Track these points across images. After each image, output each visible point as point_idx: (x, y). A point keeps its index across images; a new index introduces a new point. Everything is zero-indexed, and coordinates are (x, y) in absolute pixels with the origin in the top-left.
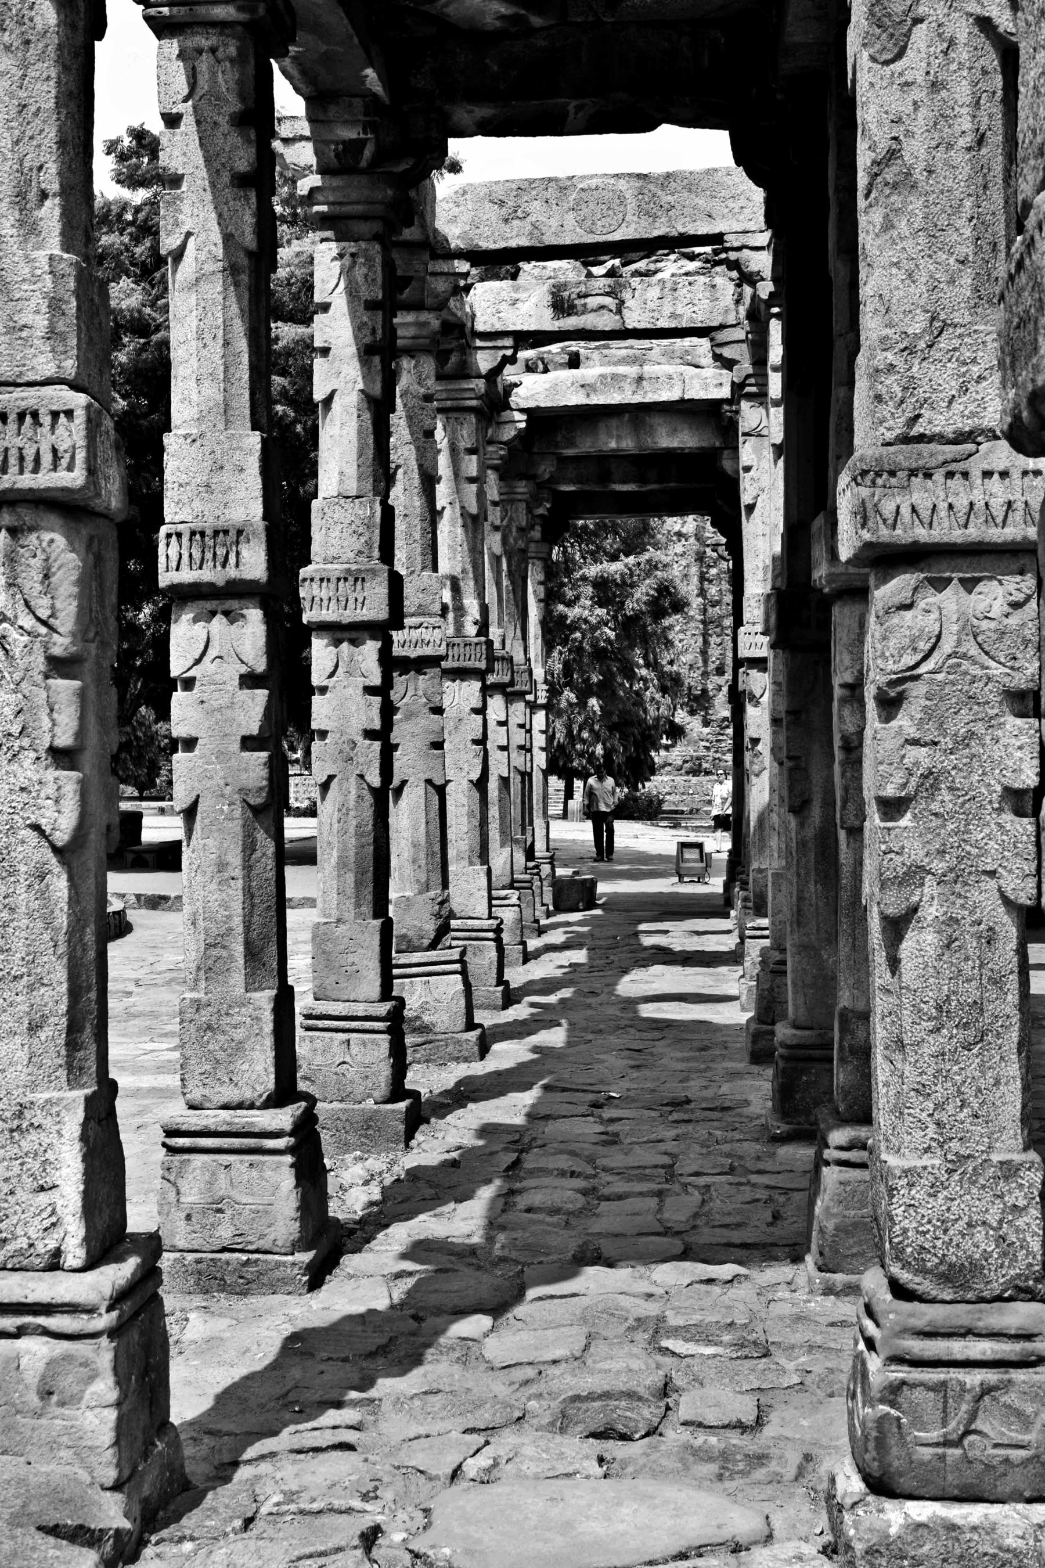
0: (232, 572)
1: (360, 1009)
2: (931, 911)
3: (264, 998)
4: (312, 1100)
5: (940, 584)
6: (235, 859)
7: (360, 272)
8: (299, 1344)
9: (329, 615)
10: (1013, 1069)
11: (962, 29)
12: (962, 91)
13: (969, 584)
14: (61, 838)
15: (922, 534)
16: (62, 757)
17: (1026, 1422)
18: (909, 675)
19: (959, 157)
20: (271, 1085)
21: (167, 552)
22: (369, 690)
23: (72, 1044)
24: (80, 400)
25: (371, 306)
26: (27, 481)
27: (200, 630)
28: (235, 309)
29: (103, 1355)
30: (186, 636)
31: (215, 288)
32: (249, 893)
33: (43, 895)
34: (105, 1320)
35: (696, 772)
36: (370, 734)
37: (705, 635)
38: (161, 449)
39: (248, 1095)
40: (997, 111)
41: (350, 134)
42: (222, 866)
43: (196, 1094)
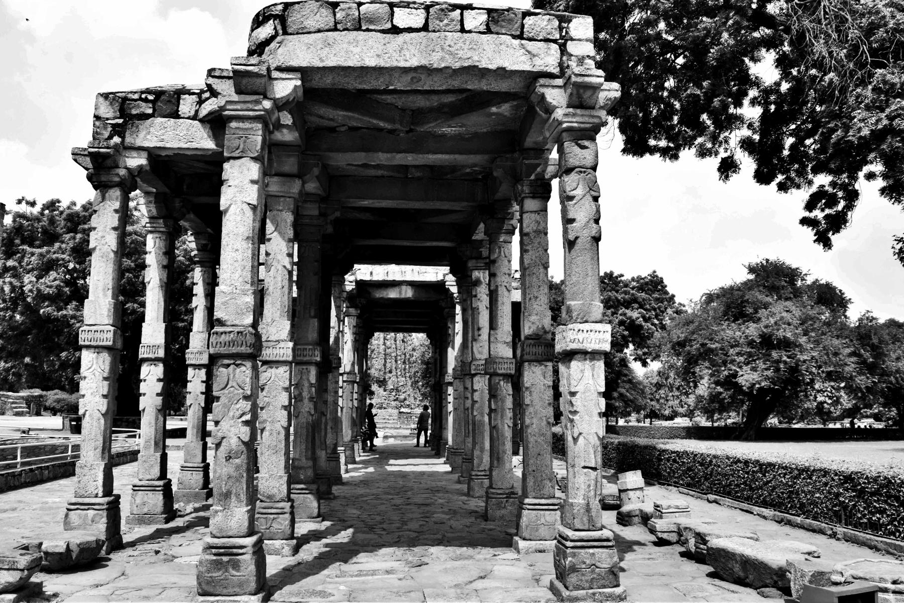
0: (156, 355)
1: (196, 465)
2: (267, 428)
3: (158, 455)
4: (170, 481)
5: (272, 368)
6: (153, 422)
7: (206, 276)
8: (158, 531)
9: (193, 362)
10: (283, 458)
11: (280, 267)
12: (280, 279)
13: (277, 368)
14: (103, 412)
15: (268, 359)
16: (104, 396)
17: (282, 525)
18: (265, 384)
19: (278, 290)
20: (158, 474)
21: (141, 350)
22: (203, 382)
23: (103, 453)
24: (112, 328)
25: (208, 284)
26: (101, 344)
27: (148, 368)
28: (161, 295)
29: (105, 513)
30: (145, 370)
31: (157, 289)
32: (156, 430)
33: (99, 423)
34: (105, 507)
35: (380, 408)
36: (202, 393)
37: (385, 359)
38: (141, 326)
39: (153, 477)
40: (287, 282)
41: (204, 242)
42: (150, 423)
43: (141, 477)
